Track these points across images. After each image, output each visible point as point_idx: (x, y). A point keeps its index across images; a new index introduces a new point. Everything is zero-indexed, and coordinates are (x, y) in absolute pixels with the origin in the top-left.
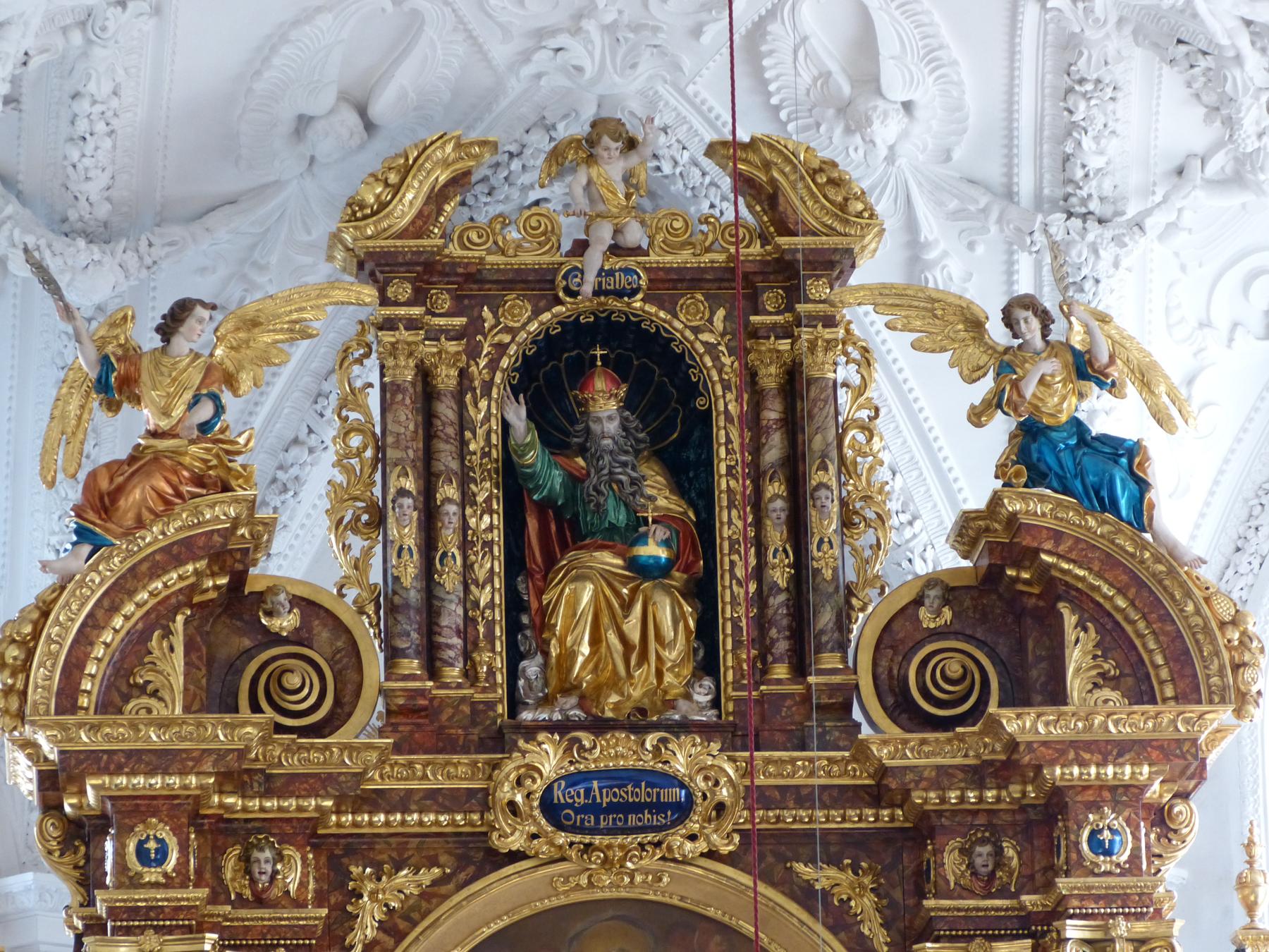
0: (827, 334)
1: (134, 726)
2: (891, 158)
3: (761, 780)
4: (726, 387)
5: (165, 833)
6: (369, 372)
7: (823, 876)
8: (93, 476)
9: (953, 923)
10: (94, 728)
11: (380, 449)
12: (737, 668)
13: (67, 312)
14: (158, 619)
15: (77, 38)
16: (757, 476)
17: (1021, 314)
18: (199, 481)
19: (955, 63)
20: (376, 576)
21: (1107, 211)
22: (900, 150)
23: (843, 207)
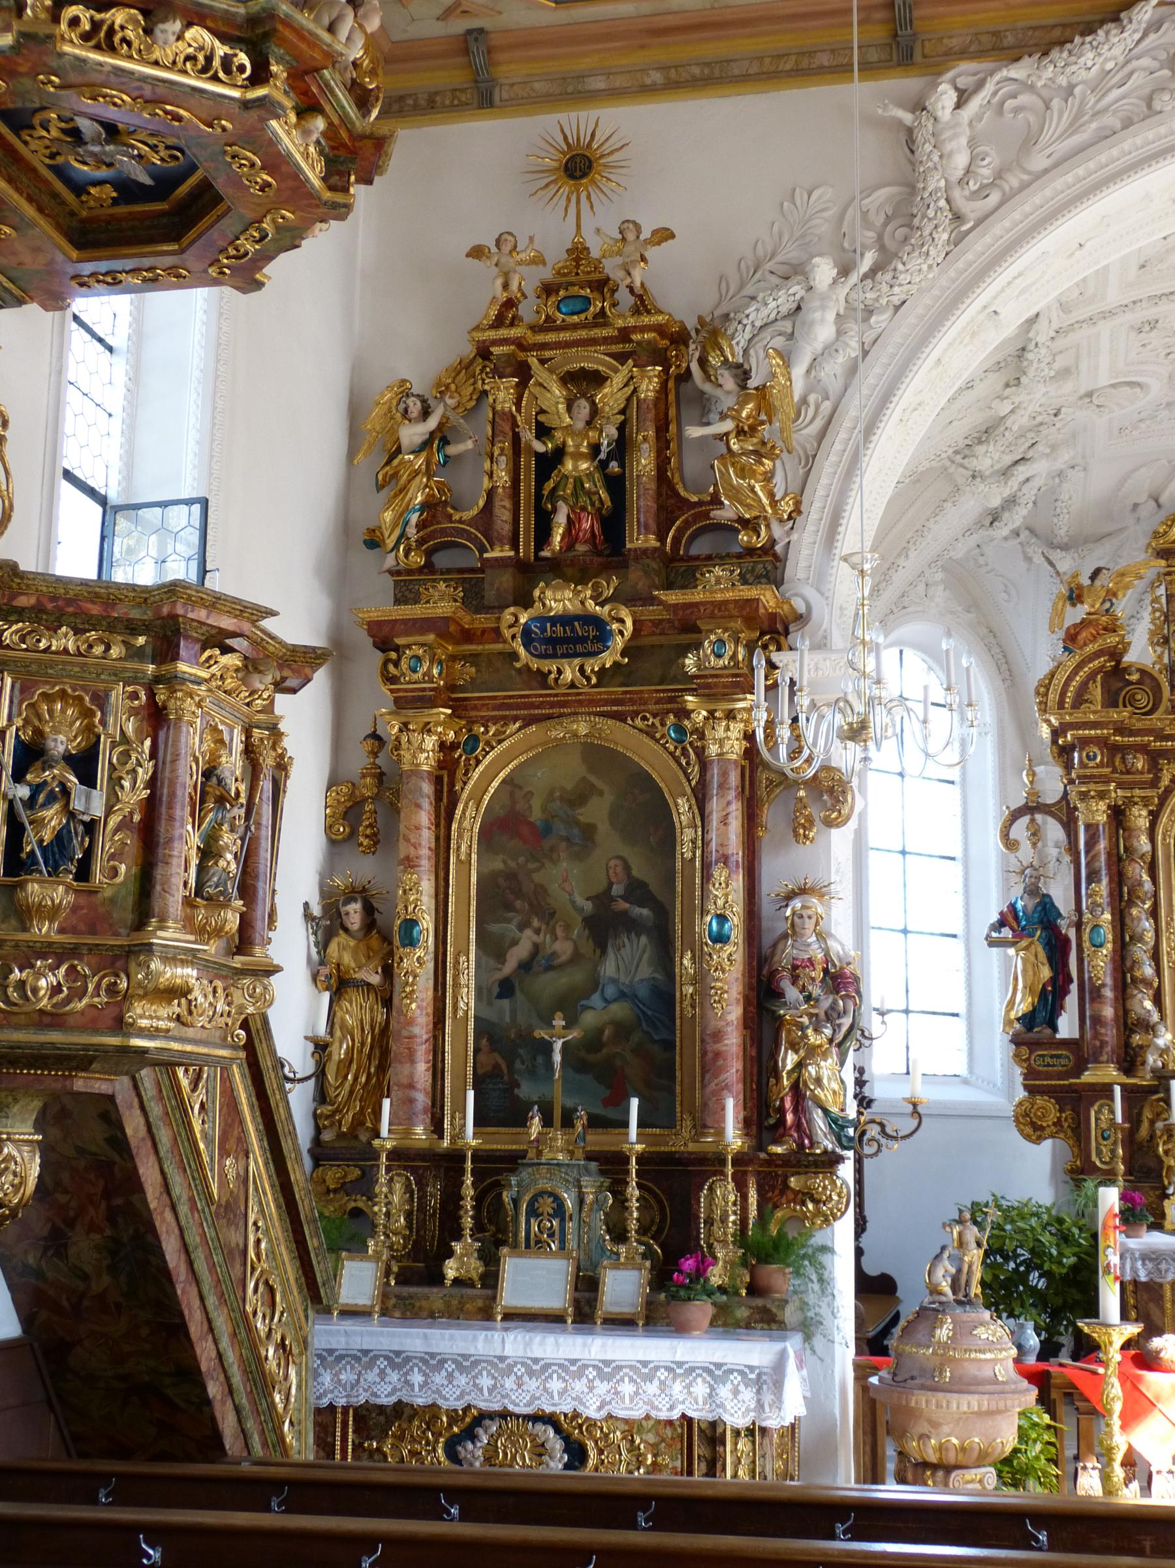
1: (1085, 713)
5: (1096, 750)
6: (1162, 590)
8: (1068, 628)
10: (1071, 714)
11: (1166, 617)
13: (1058, 573)
14: (1092, 677)
15: (1057, 480)
18: (1105, 629)
20: (1166, 660)
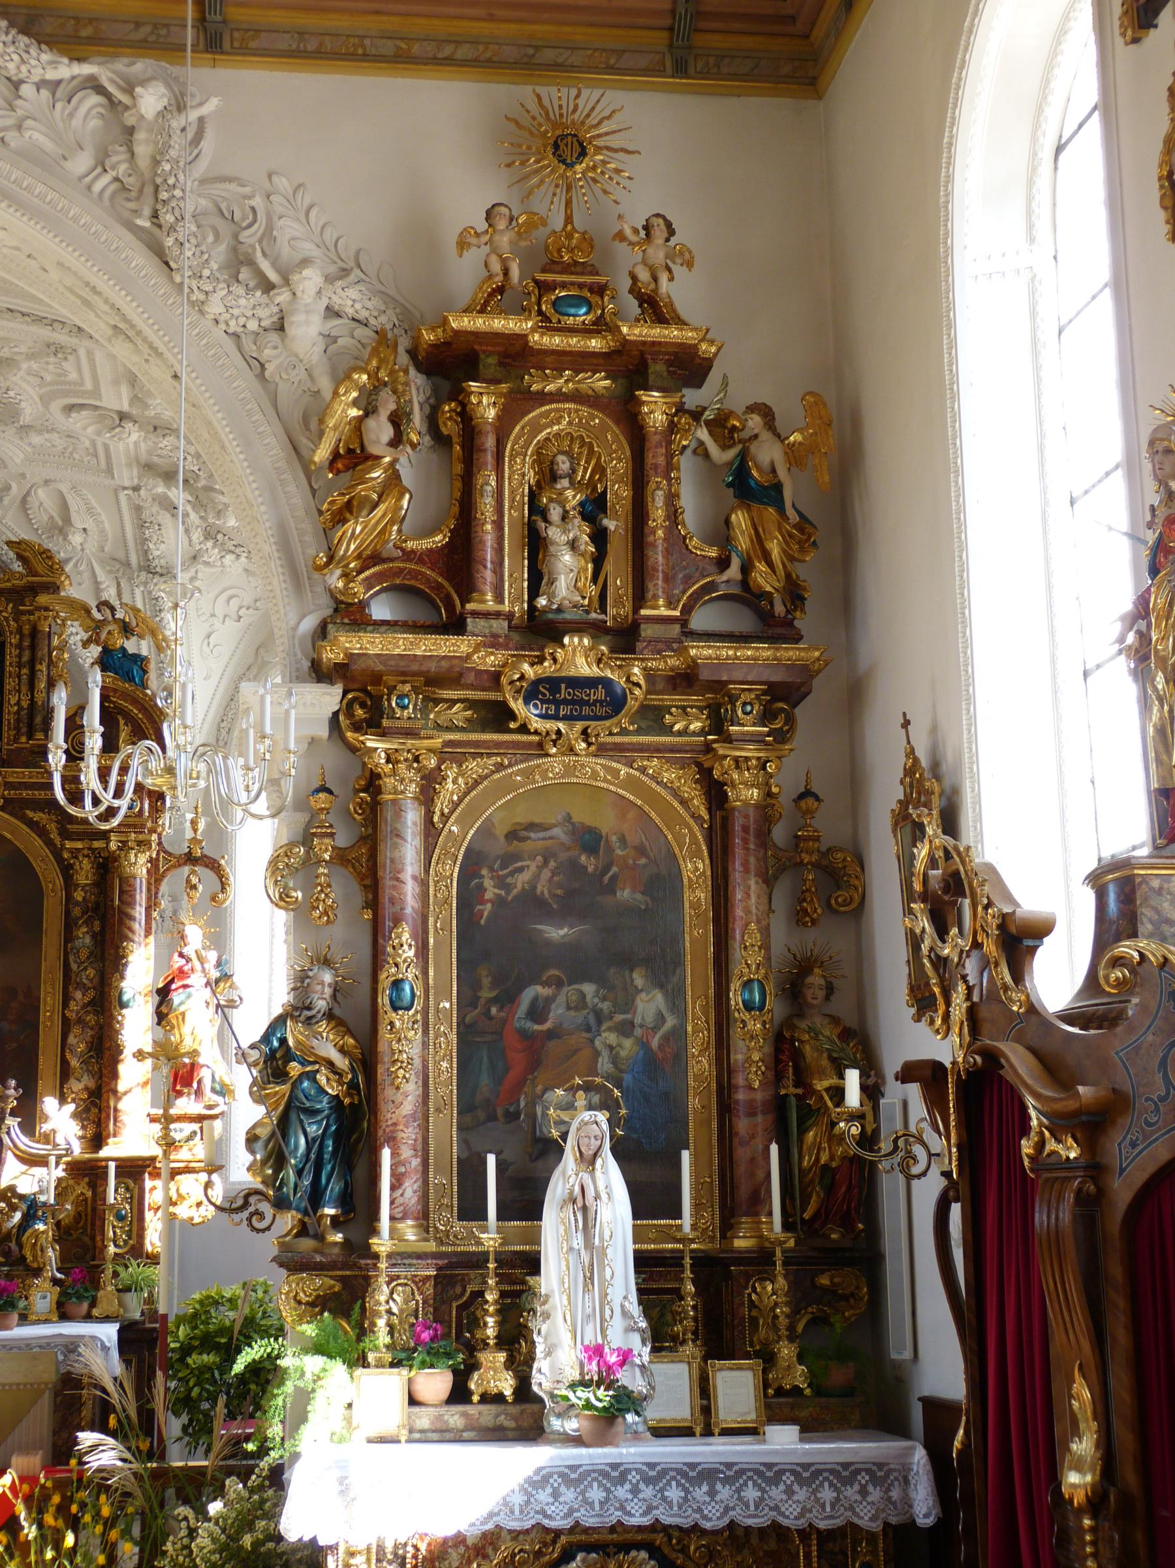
0: (45, 614)
2: (82, 550)
3: (11, 780)
4: (11, 633)
7: (36, 816)
9: (78, 834)
12: (8, 738)
16: (20, 665)
17: (102, 607)
19: (99, 514)
21: (164, 571)
22: (86, 546)
23: (51, 567)
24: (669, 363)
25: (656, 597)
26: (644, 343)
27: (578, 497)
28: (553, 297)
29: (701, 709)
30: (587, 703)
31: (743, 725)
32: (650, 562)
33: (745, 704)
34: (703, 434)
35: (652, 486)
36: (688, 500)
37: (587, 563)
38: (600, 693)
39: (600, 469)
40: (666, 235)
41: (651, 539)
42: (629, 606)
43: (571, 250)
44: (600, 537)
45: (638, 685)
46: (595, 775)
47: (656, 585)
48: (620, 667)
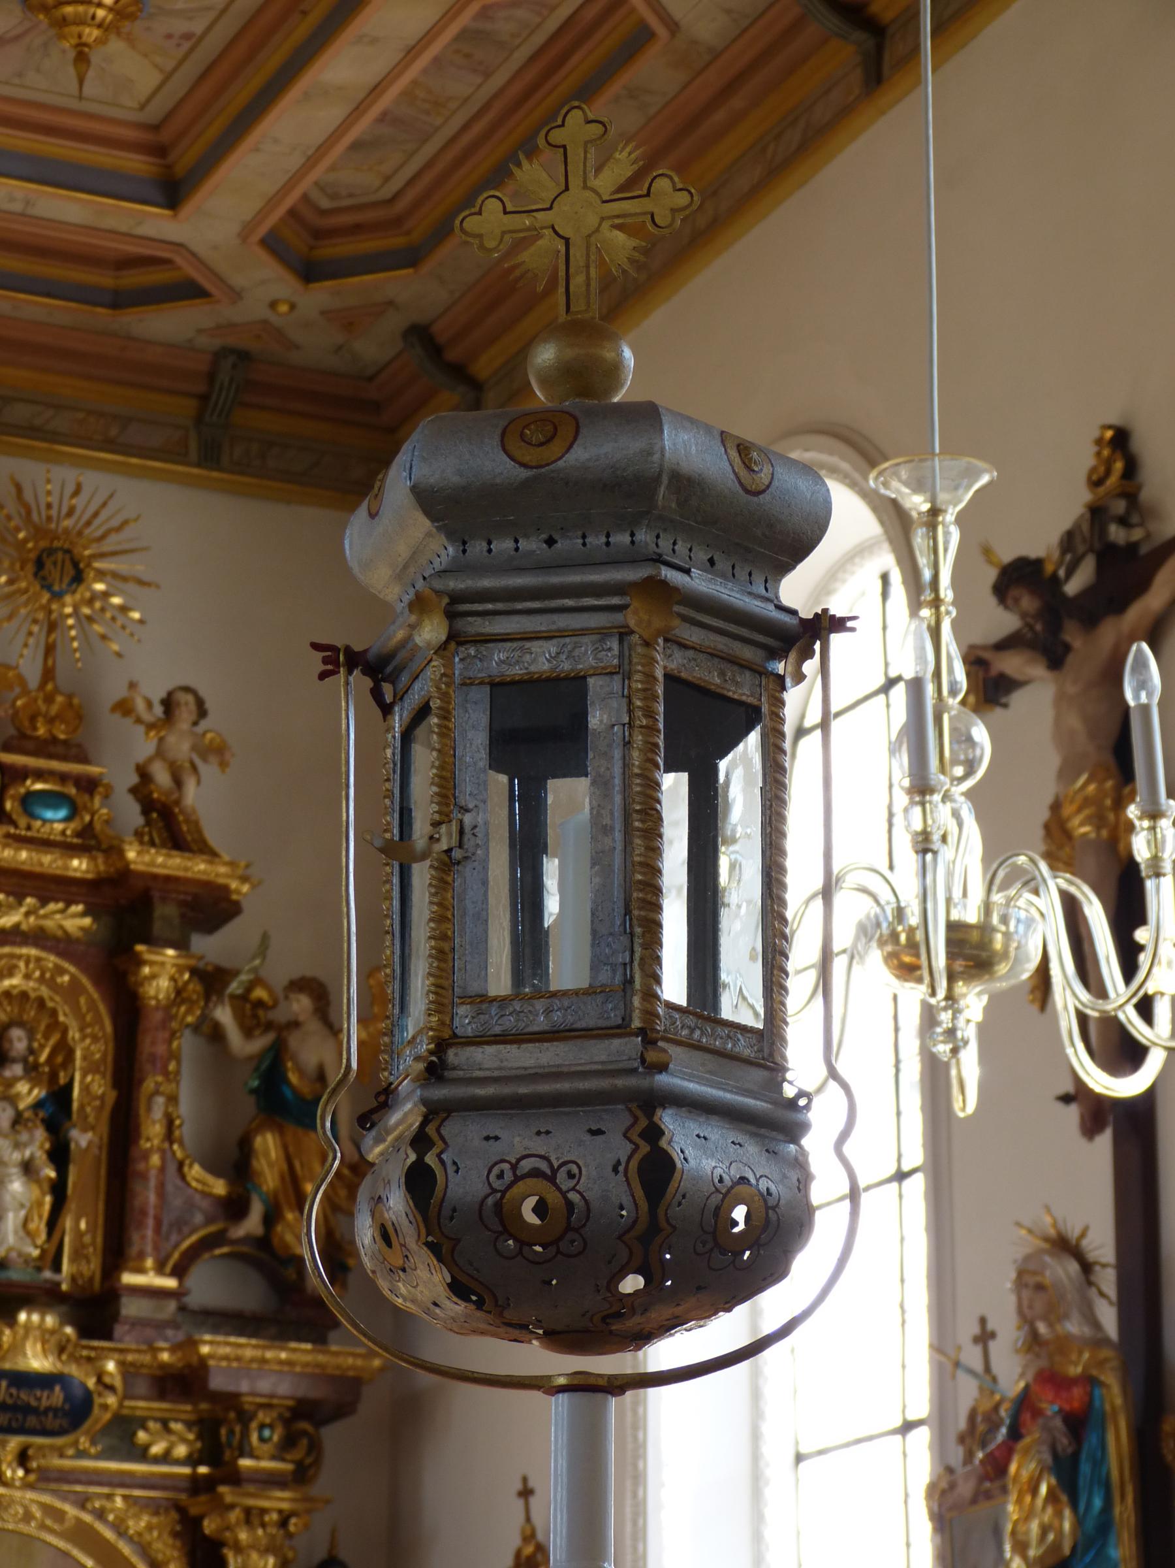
24: (183, 904)
25: (141, 1256)
26: (155, 877)
27: (36, 1092)
28: (22, 790)
29: (189, 1425)
30: (35, 1411)
31: (257, 1458)
32: (137, 1203)
33: (262, 1427)
34: (224, 1015)
35: (149, 1085)
36: (185, 1108)
37: (44, 1194)
38: (57, 1396)
39: (64, 1050)
40: (194, 717)
41: (141, 1166)
42: (93, 1267)
43: (51, 721)
44: (59, 1155)
45: (111, 1388)
46: (28, 1517)
47: (143, 1237)
48: (89, 1359)
